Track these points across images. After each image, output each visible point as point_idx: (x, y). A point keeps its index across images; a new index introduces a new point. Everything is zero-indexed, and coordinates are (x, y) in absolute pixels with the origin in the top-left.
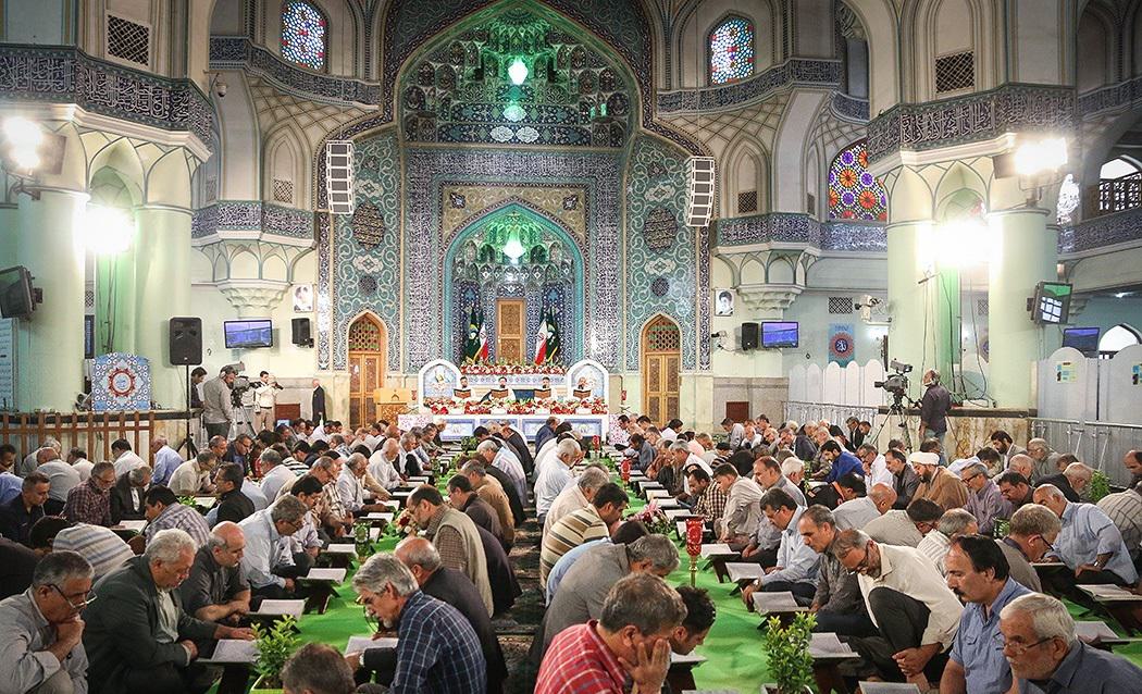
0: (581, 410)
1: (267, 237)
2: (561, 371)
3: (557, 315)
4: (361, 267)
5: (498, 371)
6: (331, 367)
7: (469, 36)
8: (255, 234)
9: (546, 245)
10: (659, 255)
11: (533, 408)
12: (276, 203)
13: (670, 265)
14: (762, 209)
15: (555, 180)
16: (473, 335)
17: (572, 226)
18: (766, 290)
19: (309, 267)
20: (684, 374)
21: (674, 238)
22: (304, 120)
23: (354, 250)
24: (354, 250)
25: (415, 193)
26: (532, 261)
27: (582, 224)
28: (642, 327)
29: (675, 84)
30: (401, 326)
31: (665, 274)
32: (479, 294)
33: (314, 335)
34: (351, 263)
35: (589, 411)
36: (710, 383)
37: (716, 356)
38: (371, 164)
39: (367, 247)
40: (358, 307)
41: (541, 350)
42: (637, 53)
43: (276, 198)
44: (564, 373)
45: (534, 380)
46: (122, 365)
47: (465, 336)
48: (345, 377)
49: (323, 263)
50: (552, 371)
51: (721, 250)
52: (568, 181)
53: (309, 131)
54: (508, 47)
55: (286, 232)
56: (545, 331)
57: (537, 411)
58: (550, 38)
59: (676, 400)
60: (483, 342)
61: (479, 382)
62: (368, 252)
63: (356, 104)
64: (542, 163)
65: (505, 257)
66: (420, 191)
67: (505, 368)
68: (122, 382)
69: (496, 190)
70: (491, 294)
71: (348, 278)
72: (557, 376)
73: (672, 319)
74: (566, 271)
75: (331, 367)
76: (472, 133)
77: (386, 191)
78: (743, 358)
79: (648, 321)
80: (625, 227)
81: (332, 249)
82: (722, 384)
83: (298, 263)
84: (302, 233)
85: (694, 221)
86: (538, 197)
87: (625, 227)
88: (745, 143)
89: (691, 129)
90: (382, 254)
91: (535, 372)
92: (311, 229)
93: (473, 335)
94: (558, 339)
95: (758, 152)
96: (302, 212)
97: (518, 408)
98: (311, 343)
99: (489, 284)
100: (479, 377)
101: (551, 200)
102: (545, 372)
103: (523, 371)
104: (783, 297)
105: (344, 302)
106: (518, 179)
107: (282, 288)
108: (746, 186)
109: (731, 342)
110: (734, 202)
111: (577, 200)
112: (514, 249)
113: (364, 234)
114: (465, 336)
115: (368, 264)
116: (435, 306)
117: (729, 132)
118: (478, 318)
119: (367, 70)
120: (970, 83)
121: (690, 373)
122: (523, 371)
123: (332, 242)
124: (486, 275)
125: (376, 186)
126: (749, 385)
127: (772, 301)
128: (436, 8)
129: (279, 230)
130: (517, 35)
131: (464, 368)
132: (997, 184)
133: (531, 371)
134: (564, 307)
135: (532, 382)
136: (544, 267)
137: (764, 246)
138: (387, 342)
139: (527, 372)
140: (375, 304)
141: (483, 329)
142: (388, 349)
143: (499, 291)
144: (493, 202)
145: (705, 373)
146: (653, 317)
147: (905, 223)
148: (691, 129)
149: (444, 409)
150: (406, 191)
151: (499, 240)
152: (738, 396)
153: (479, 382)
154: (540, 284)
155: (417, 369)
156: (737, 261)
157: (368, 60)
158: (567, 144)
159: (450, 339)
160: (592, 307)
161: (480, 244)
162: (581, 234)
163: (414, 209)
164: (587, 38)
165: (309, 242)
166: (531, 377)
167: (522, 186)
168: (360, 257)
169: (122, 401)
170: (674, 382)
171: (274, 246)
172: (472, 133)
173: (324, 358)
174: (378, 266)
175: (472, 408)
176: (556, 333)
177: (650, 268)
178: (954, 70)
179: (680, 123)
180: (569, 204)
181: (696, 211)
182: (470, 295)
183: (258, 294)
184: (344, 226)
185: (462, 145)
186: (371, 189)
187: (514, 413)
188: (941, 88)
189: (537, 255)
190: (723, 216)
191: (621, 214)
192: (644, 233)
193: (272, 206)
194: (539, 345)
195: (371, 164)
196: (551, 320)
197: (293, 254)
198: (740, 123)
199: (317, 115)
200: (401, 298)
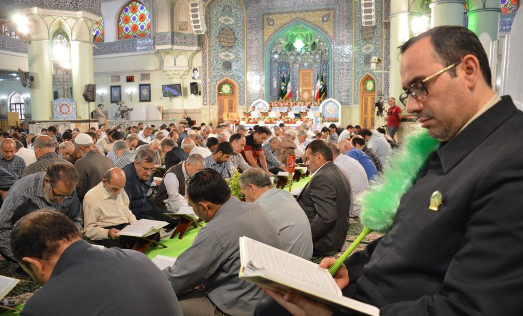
1: (175, 47)
2: (317, 105)
4: (223, 58)
5: (287, 104)
6: (208, 104)
8: (169, 46)
9: (317, 41)
12: (180, 32)
15: (318, 7)
16: (283, 88)
17: (327, 30)
21: (374, 32)
23: (219, 50)
24: (219, 50)
25: (251, 21)
28: (360, 81)
31: (370, 52)
32: (289, 67)
33: (201, 89)
34: (218, 56)
38: (227, 9)
39: (226, 48)
43: (180, 29)
44: (318, 105)
48: (215, 108)
49: (204, 57)
52: (324, 7)
55: (185, 44)
56: (319, 85)
60: (289, 91)
62: (226, 50)
66: (253, 19)
69: (289, 15)
71: (217, 63)
72: (315, 107)
73: (373, 77)
75: (208, 104)
77: (236, 21)
79: (363, 78)
80: (354, 29)
81: (208, 51)
84: (192, 45)
85: (366, 23)
86: (310, 17)
87: (354, 29)
90: (234, 51)
92: (196, 42)
97: (271, 121)
99: (294, 62)
100: (277, 108)
103: (299, 105)
105: (214, 74)
106: (299, 9)
107: (186, 69)
111: (329, 16)
112: (299, 44)
113: (225, 42)
123: (207, 47)
125: (231, 19)
129: (181, 44)
138: (238, 92)
140: (231, 74)
141: (289, 84)
143: (300, 65)
144: (287, 22)
146: (364, 76)
150: (247, 20)
154: (319, 61)
160: (336, 72)
161: (284, 43)
163: (251, 28)
167: (301, 12)
168: (223, 53)
171: (180, 52)
173: (205, 99)
174: (232, 56)
175: (251, 121)
180: (325, 19)
181: (366, 17)
183: (176, 73)
184: (239, 38)
186: (228, 21)
191: (352, 22)
193: (177, 33)
195: (227, 9)
197: (189, 54)
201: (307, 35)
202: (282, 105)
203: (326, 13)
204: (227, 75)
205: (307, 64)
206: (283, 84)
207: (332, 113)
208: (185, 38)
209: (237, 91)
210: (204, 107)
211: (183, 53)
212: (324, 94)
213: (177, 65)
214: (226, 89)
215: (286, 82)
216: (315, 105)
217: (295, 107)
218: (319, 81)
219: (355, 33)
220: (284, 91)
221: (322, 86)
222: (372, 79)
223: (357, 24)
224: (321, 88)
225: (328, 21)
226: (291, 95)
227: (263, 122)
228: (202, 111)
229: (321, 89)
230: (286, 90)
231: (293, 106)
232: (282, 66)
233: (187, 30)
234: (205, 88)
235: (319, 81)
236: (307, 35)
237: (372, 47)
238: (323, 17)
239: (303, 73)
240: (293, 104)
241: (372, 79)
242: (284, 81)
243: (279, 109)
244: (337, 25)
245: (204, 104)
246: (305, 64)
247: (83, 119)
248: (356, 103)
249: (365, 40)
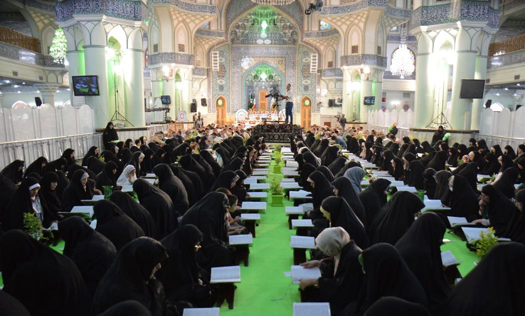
4: (219, 83)
7: (250, 14)
9: (273, 75)
10: (307, 79)
13: (309, 82)
14: (334, 67)
16: (251, 102)
18: (335, 90)
19: (205, 83)
20: (312, 114)
22: (203, 43)
26: (269, 79)
27: (284, 69)
29: (310, 30)
33: (207, 103)
36: (319, 116)
37: (321, 109)
40: (218, 94)
42: (299, 20)
46: (182, 113)
47: (249, 102)
49: (209, 82)
51: (323, 78)
53: (205, 46)
54: (261, 15)
55: (200, 75)
58: (274, 14)
59: (310, 121)
60: (254, 104)
62: (221, 78)
63: (218, 37)
64: (272, 51)
65: (261, 79)
66: (236, 59)
68: (182, 116)
69: (258, 59)
70: (257, 89)
74: (279, 83)
76: (251, 42)
78: (330, 109)
82: (323, 117)
83: (202, 83)
84: (203, 75)
88: (330, 47)
89: (315, 42)
92: (206, 73)
95: (333, 50)
96: (203, 69)
98: (206, 105)
99: (256, 86)
101: (273, 63)
104: (340, 92)
107: (198, 90)
108: (330, 60)
109: (327, 105)
110: (327, 64)
114: (249, 102)
115: (221, 82)
116: (240, 93)
117: (325, 44)
118: (253, 97)
119: (221, 27)
120: (357, 52)
121: (314, 113)
124: (255, 83)
126: (331, 117)
127: (337, 93)
128: (240, 8)
130: (264, 12)
132: (362, 74)
136: (273, 81)
137: (334, 78)
141: (255, 100)
142: (227, 107)
145: (318, 114)
147: (346, 81)
148: (315, 42)
151: (259, 73)
152: (328, 120)
155: (235, 112)
156: (327, 81)
157: (221, 24)
158: (280, 44)
159: (245, 103)
161: (253, 74)
162: (284, 72)
164: (285, 15)
165: (205, 77)
167: (265, 57)
169: (182, 120)
170: (310, 116)
172: (251, 42)
174: (224, 82)
177: (303, 82)
178: (355, 49)
179: (311, 41)
180: (280, 63)
182: (251, 89)
185: (248, 45)
188: (352, 52)
189: (271, 77)
190: (323, 68)
192: (302, 72)
194: (272, 104)
197: (201, 80)
198: (328, 42)
199: (207, 41)
201: (266, 70)
203: (281, 59)
204: (221, 94)
206: (252, 99)
208: (200, 71)
209: (226, 104)
210: (209, 114)
211: (198, 80)
213: (194, 86)
214: (220, 102)
219: (298, 72)
222: (309, 99)
223: (299, 67)
225: (281, 64)
226: (255, 106)
228: (208, 116)
233: (200, 66)
234: (209, 102)
236: (266, 70)
237: (309, 82)
238: (279, 61)
241: (309, 99)
242: (252, 98)
244: (287, 67)
245: (209, 112)
247: (190, 122)
248: (298, 112)
249: (304, 77)
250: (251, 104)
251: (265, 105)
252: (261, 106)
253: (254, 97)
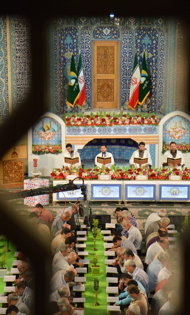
0: (173, 177)
2: (153, 122)
3: (150, 60)
5: (99, 122)
11: (134, 175)
30: (9, 79)
35: (179, 177)
41: (134, 94)
44: (157, 123)
45: (130, 130)
50: (146, 122)
56: (138, 76)
57: (138, 177)
60: (81, 86)
61: (82, 132)
67: (103, 120)
72: (151, 126)
91: (130, 123)
93: (73, 82)
94: (150, 83)
100: (82, 128)
102: (139, 123)
103: (120, 122)
122: (120, 122)
131: (68, 120)
133: (127, 122)
134: (156, 53)
135: (128, 132)
139: (123, 123)
141: (81, 74)
149: (61, 175)
153: (82, 132)
166: (127, 127)
176: (149, 78)
187: (119, 179)
194: (133, 88)
196: (145, 65)
200: (9, 53)
202: (89, 123)
205: (109, 31)
206: (73, 74)
207: (178, 135)
212: (148, 93)
215: (76, 69)
216: (150, 123)
217: (114, 127)
218: (138, 70)
220: (75, 87)
221: (143, 79)
224: (143, 81)
227: (108, 177)
229: (141, 85)
230: (78, 86)
231: (110, 125)
232: (66, 36)
235: (138, 70)
239: (98, 48)
240: (111, 122)
243: (84, 130)
246: (104, 31)
250: (71, 87)
251: (110, 87)
252: (101, 88)
253: (79, 69)
